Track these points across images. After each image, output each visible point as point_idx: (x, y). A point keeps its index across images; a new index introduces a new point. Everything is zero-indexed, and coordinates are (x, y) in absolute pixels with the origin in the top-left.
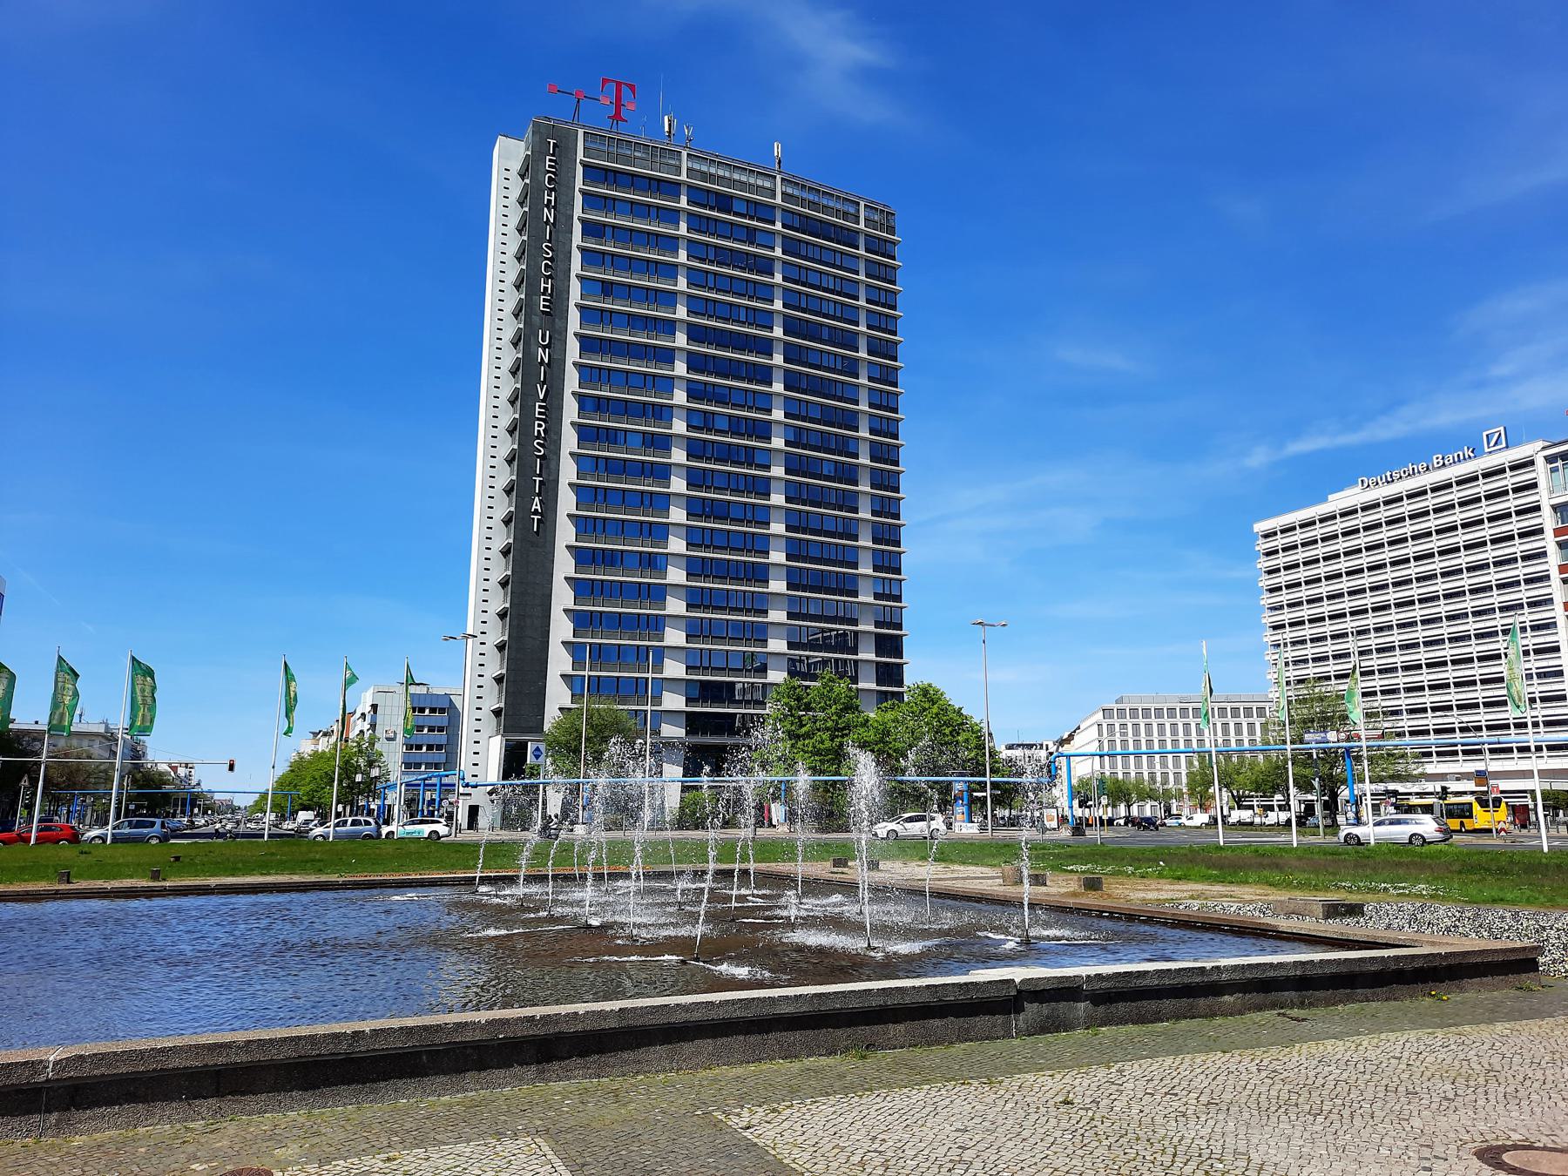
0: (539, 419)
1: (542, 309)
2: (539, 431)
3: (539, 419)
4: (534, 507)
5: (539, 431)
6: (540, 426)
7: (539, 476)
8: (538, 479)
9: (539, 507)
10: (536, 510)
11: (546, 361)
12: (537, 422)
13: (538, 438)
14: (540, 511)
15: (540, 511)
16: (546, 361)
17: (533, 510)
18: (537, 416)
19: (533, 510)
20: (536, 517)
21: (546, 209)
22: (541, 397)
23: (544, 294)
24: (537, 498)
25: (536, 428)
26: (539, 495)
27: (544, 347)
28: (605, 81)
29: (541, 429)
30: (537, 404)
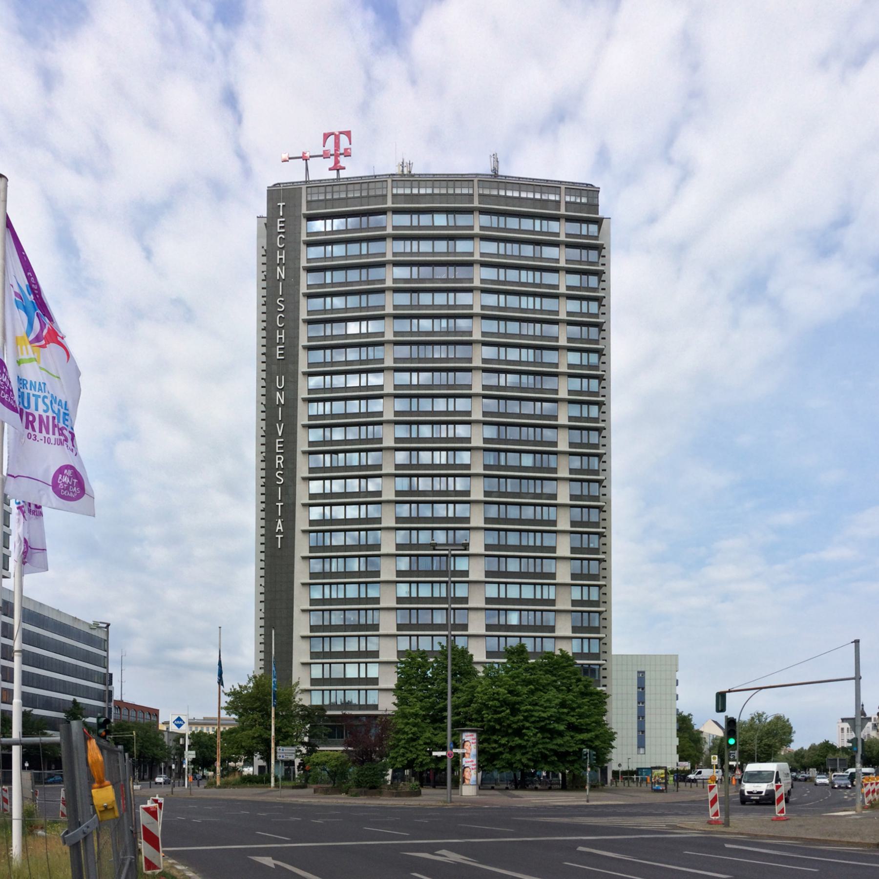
0: (279, 453)
1: (278, 357)
2: (279, 463)
3: (279, 453)
4: (278, 528)
5: (279, 463)
6: (280, 459)
7: (281, 501)
8: (279, 504)
9: (281, 528)
10: (279, 530)
11: (283, 402)
12: (277, 456)
13: (278, 469)
14: (282, 531)
15: (282, 531)
16: (283, 402)
17: (277, 531)
18: (277, 451)
19: (277, 531)
20: (279, 536)
21: (278, 268)
22: (280, 434)
23: (279, 344)
24: (279, 520)
25: (277, 462)
26: (280, 517)
27: (280, 390)
28: (326, 136)
29: (281, 462)
30: (277, 440)
